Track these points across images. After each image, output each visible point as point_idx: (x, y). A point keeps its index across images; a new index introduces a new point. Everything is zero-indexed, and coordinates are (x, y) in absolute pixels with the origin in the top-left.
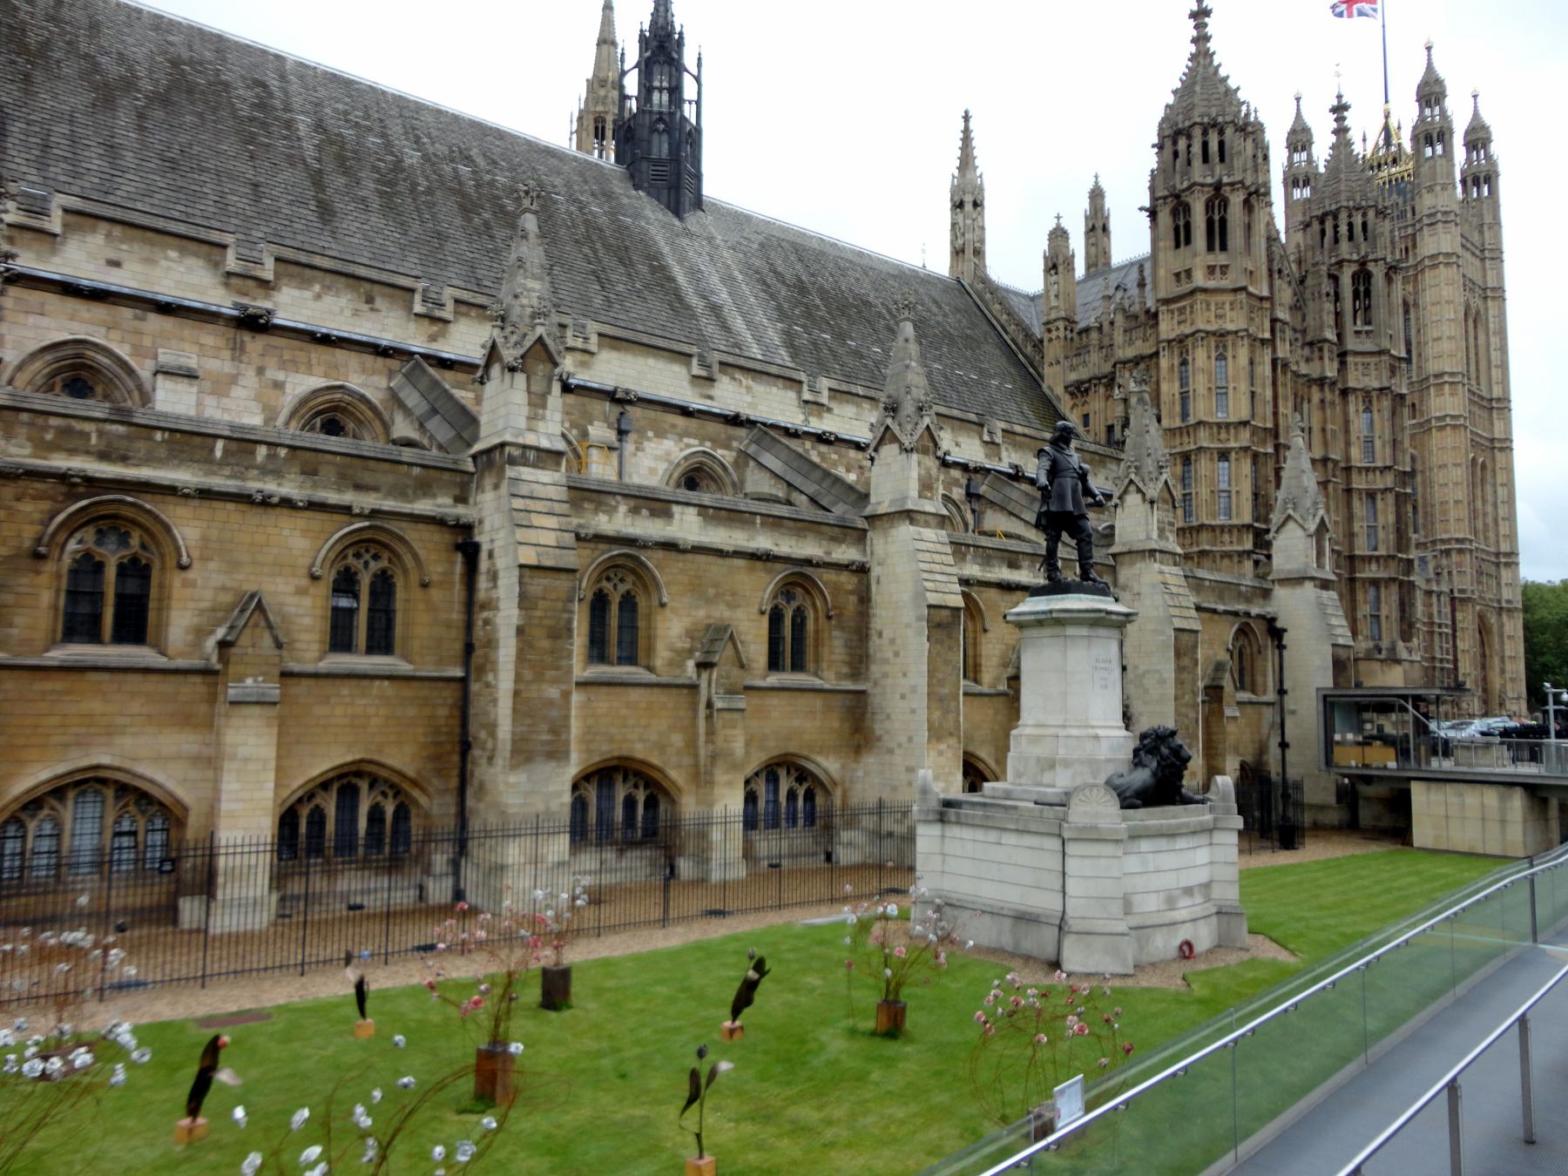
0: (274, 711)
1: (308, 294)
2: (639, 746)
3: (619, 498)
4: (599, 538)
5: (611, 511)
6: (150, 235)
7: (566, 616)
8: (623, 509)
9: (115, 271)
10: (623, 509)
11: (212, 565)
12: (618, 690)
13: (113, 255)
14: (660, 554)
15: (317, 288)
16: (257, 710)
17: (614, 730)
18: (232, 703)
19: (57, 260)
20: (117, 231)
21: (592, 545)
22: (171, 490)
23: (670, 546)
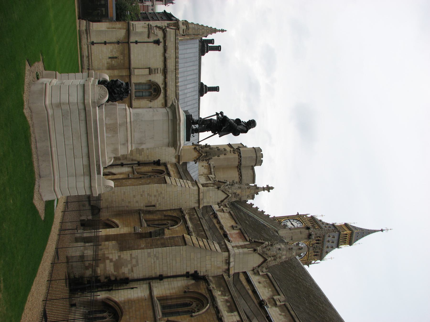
0: (133, 232)
1: (280, 313)
2: (128, 317)
3: (230, 296)
4: (210, 291)
5: (223, 294)
6: (272, 286)
7: (170, 245)
8: (226, 298)
9: (258, 284)
10: (226, 298)
11: (170, 232)
12: (151, 307)
13: (261, 282)
14: (213, 312)
15: (284, 314)
16: (133, 230)
17: (134, 308)
18: (134, 227)
19: (253, 276)
20: (268, 281)
21: (207, 292)
22: (185, 222)
23: (218, 311)
